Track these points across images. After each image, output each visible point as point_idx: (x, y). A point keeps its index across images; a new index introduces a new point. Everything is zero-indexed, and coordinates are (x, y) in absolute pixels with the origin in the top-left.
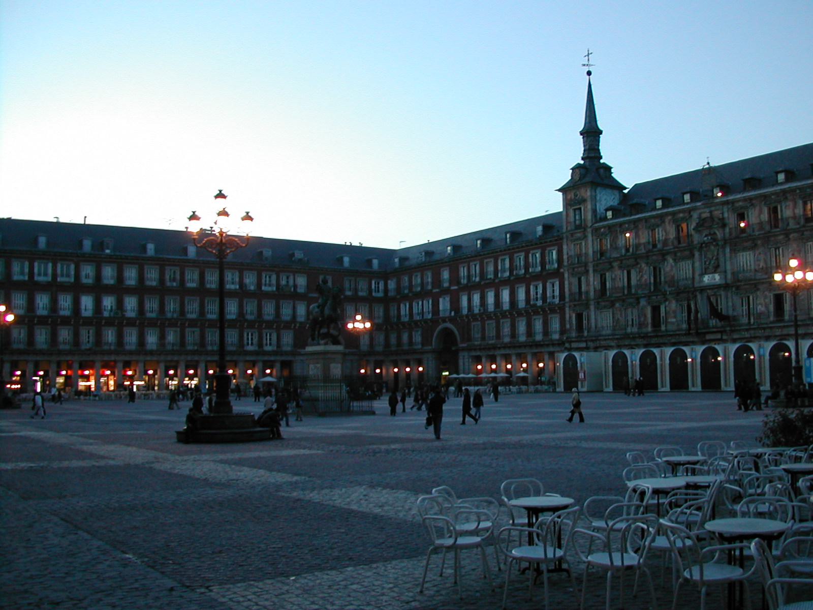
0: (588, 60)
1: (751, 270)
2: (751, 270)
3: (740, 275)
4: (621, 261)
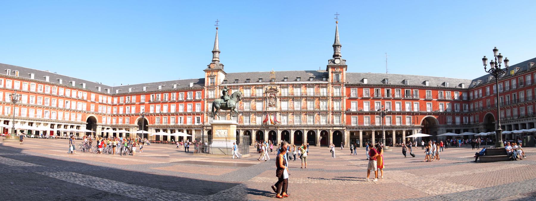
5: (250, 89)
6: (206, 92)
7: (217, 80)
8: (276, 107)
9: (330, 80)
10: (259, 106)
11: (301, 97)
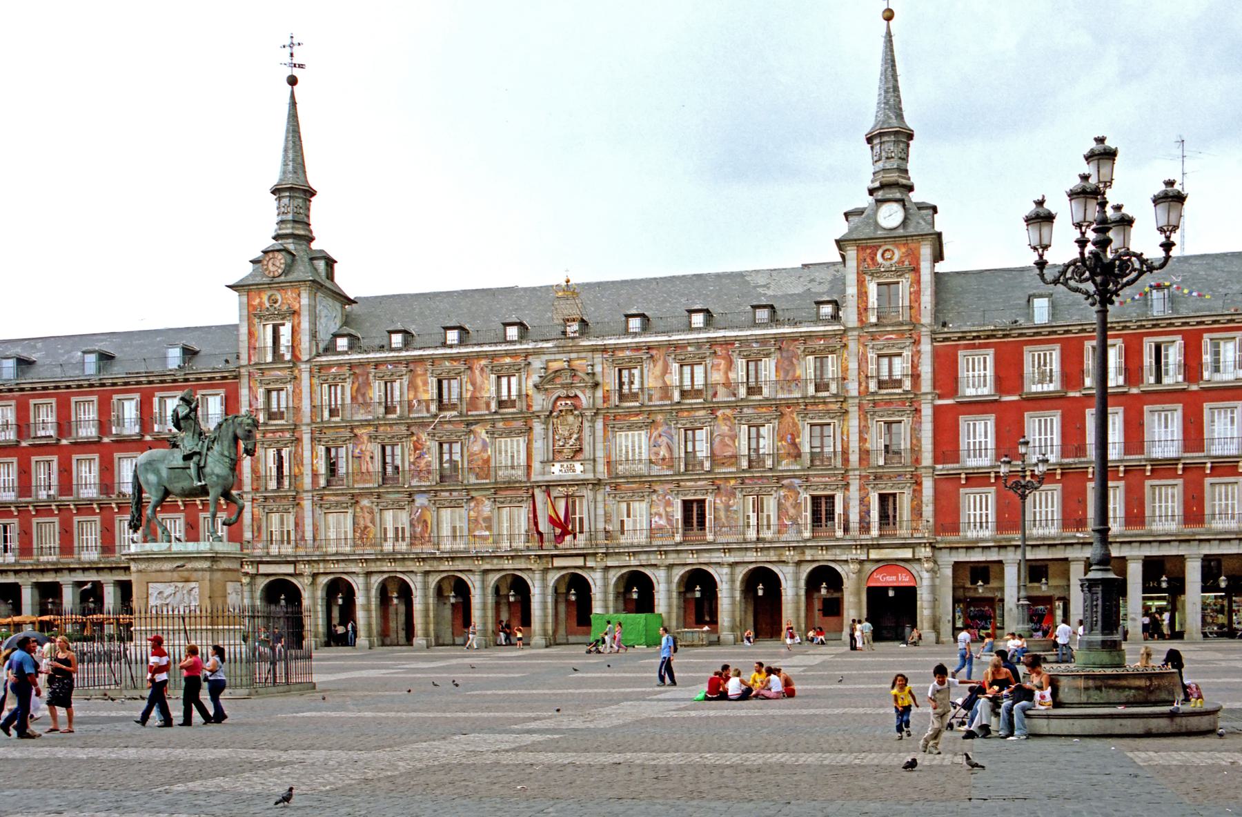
1: (640, 460)
2: (640, 460)
3: (620, 468)
4: (377, 427)
9: (850, 316)
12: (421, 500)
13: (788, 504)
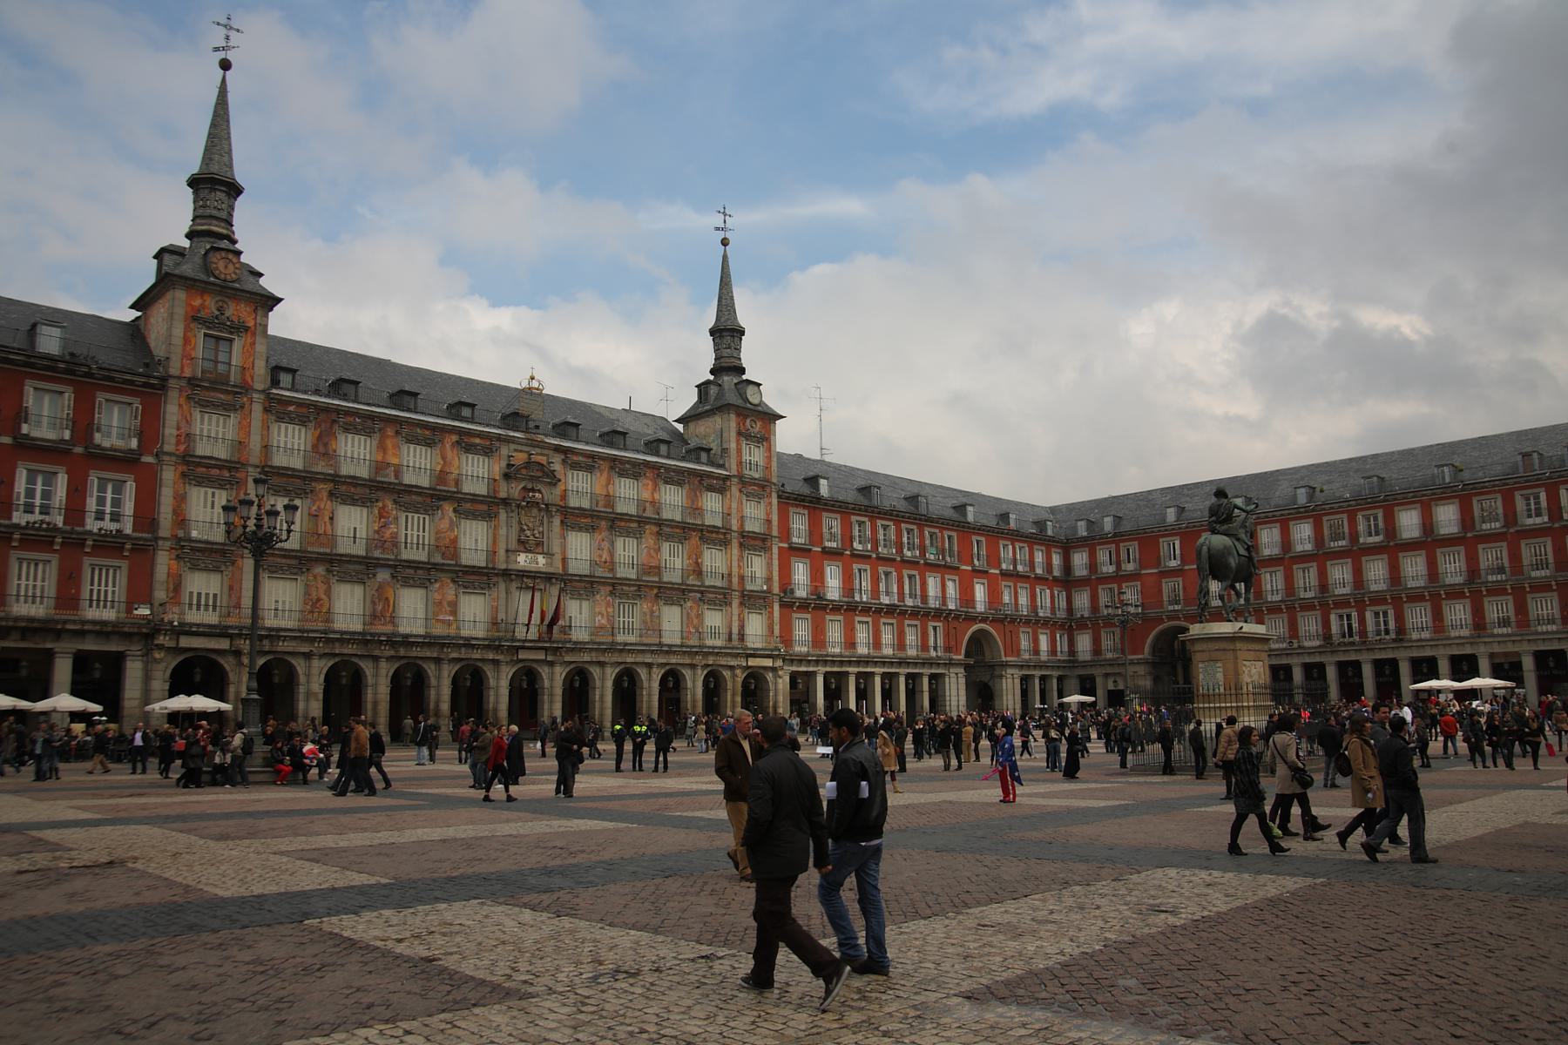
0: (227, 38)
5: (429, 444)
6: (172, 411)
7: (249, 351)
8: (549, 555)
10: (474, 541)
11: (642, 521)
12: (383, 575)
13: (693, 615)
